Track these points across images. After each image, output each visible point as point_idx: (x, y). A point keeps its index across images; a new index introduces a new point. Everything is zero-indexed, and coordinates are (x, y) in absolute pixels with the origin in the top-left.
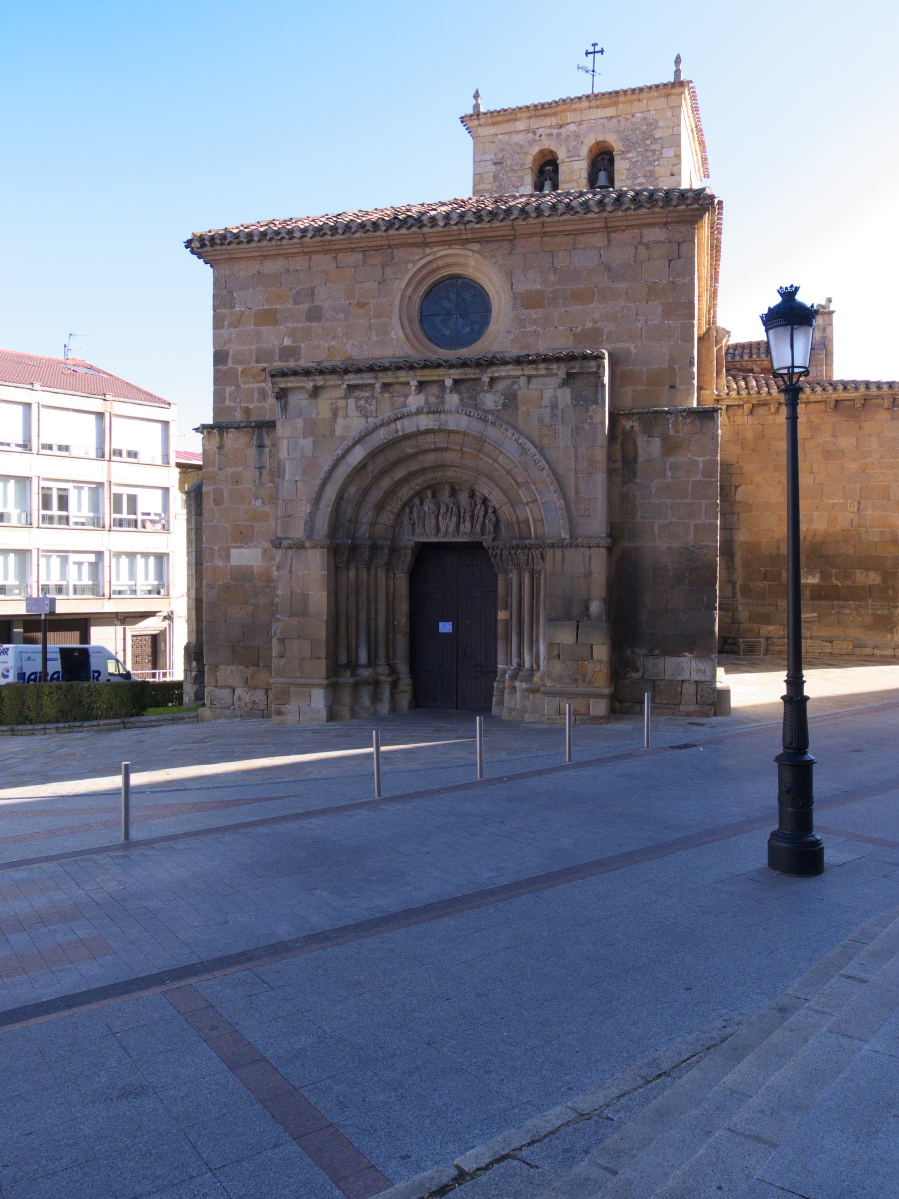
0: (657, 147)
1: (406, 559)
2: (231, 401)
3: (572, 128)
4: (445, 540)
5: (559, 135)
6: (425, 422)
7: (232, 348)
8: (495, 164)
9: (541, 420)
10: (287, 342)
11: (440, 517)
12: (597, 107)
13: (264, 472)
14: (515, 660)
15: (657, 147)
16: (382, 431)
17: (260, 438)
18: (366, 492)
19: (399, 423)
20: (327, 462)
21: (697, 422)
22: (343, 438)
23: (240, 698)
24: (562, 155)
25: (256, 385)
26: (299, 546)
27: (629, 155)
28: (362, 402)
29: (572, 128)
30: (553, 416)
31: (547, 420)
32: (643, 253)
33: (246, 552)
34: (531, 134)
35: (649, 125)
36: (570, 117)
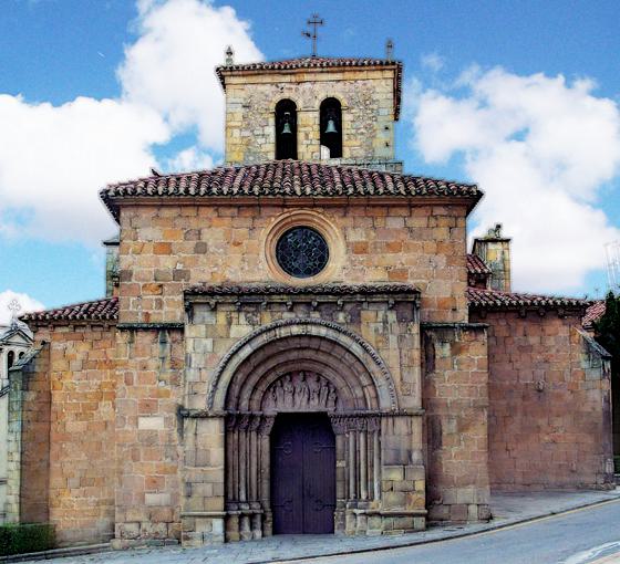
0: (375, 107)
1: (270, 423)
2: (134, 307)
5: (297, 90)
6: (296, 330)
7: (136, 269)
9: (376, 330)
10: (179, 267)
11: (296, 395)
12: (328, 72)
14: (352, 495)
15: (375, 107)
16: (264, 335)
18: (248, 376)
19: (277, 330)
20: (224, 353)
21: (473, 334)
23: (145, 531)
24: (300, 105)
25: (154, 297)
26: (202, 416)
27: (353, 111)
28: (250, 315)
29: (308, 85)
30: (385, 328)
31: (381, 331)
32: (433, 222)
36: (307, 77)
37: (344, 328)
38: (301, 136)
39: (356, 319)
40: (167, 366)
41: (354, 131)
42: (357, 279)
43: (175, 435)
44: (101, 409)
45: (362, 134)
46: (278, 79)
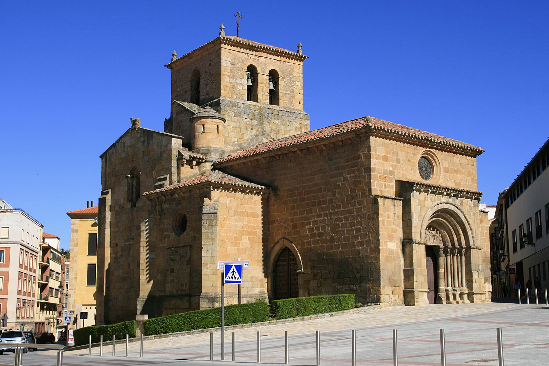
0: (294, 80)
4: (432, 244)
5: (258, 60)
7: (376, 167)
10: (391, 169)
13: (396, 215)
17: (394, 203)
22: (428, 208)
24: (259, 71)
25: (384, 183)
27: (284, 80)
37: (460, 207)
38: (259, 89)
39: (462, 204)
40: (396, 218)
41: (285, 92)
42: (446, 184)
44: (243, 240)
45: (289, 94)
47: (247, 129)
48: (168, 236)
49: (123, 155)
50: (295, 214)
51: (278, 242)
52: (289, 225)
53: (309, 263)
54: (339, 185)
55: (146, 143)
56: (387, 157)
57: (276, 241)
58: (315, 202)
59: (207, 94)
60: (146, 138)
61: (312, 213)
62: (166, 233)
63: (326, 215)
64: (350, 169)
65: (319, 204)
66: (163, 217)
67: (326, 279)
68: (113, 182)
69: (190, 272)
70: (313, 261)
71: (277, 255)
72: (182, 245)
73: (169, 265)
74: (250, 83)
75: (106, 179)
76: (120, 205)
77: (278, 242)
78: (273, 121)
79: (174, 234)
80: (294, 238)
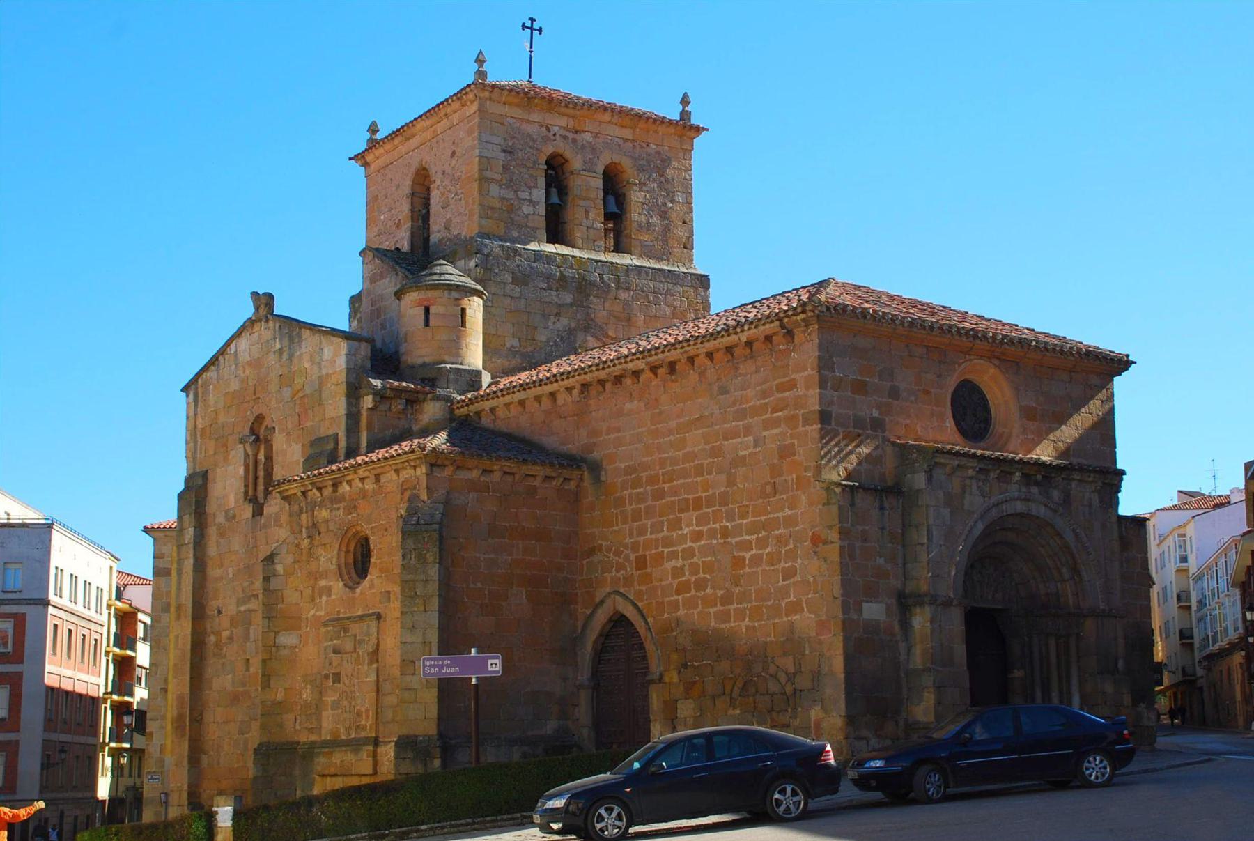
3: (588, 137)
5: (574, 141)
6: (1020, 507)
7: (835, 410)
8: (504, 151)
10: (875, 414)
17: (881, 501)
24: (576, 163)
29: (588, 137)
33: (874, 606)
34: (544, 129)
35: (663, 161)
43: (897, 628)
46: (550, 119)
47: (545, 316)
48: (328, 591)
49: (235, 386)
50: (642, 531)
51: (602, 602)
52: (627, 559)
53: (675, 656)
54: (744, 456)
55: (285, 356)
56: (864, 383)
57: (598, 600)
58: (687, 500)
59: (447, 228)
60: (286, 342)
61: (681, 529)
62: (323, 583)
63: (712, 534)
64: (768, 415)
65: (697, 505)
66: (316, 543)
67: (714, 697)
68: (211, 452)
69: (378, 681)
70: (684, 650)
71: (601, 635)
72: (360, 613)
73: (330, 664)
74: (555, 199)
75: (196, 442)
76: (226, 512)
77: (602, 602)
78: (612, 295)
79: (341, 584)
80: (640, 591)
